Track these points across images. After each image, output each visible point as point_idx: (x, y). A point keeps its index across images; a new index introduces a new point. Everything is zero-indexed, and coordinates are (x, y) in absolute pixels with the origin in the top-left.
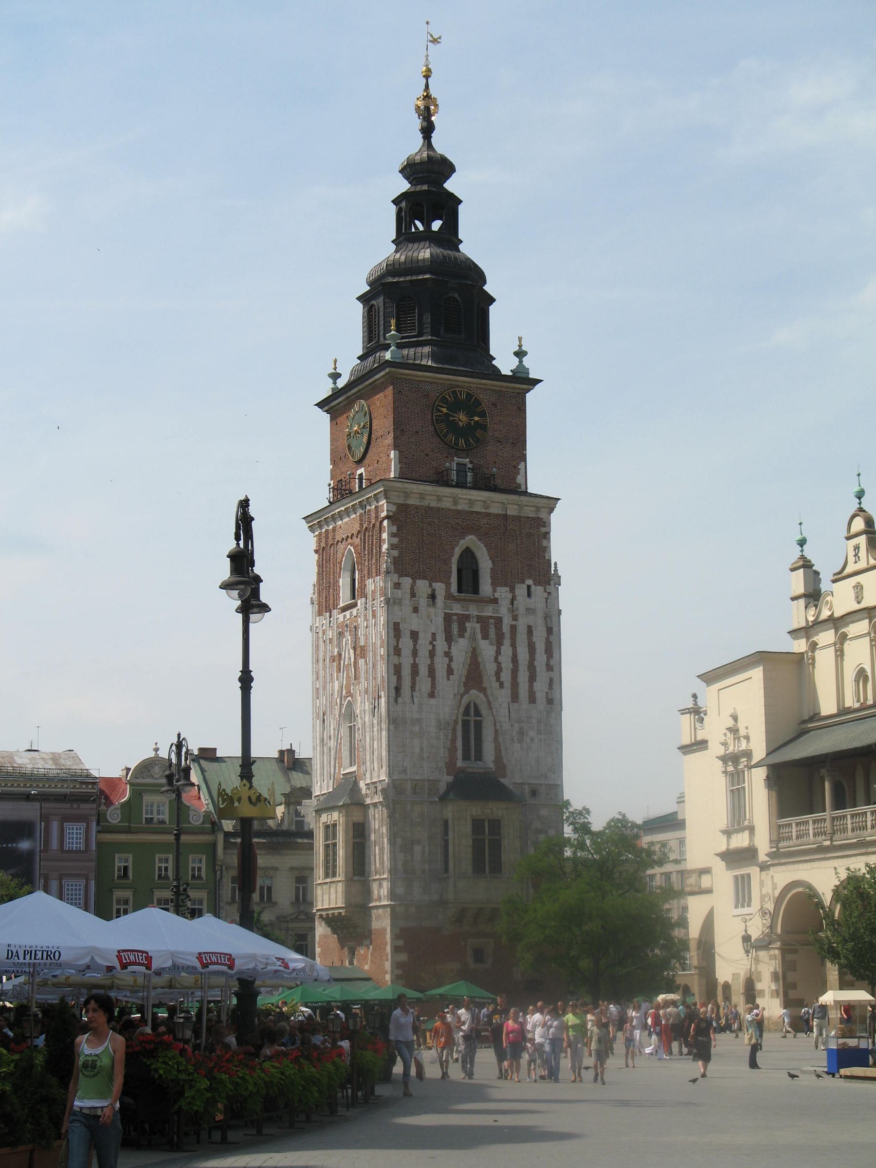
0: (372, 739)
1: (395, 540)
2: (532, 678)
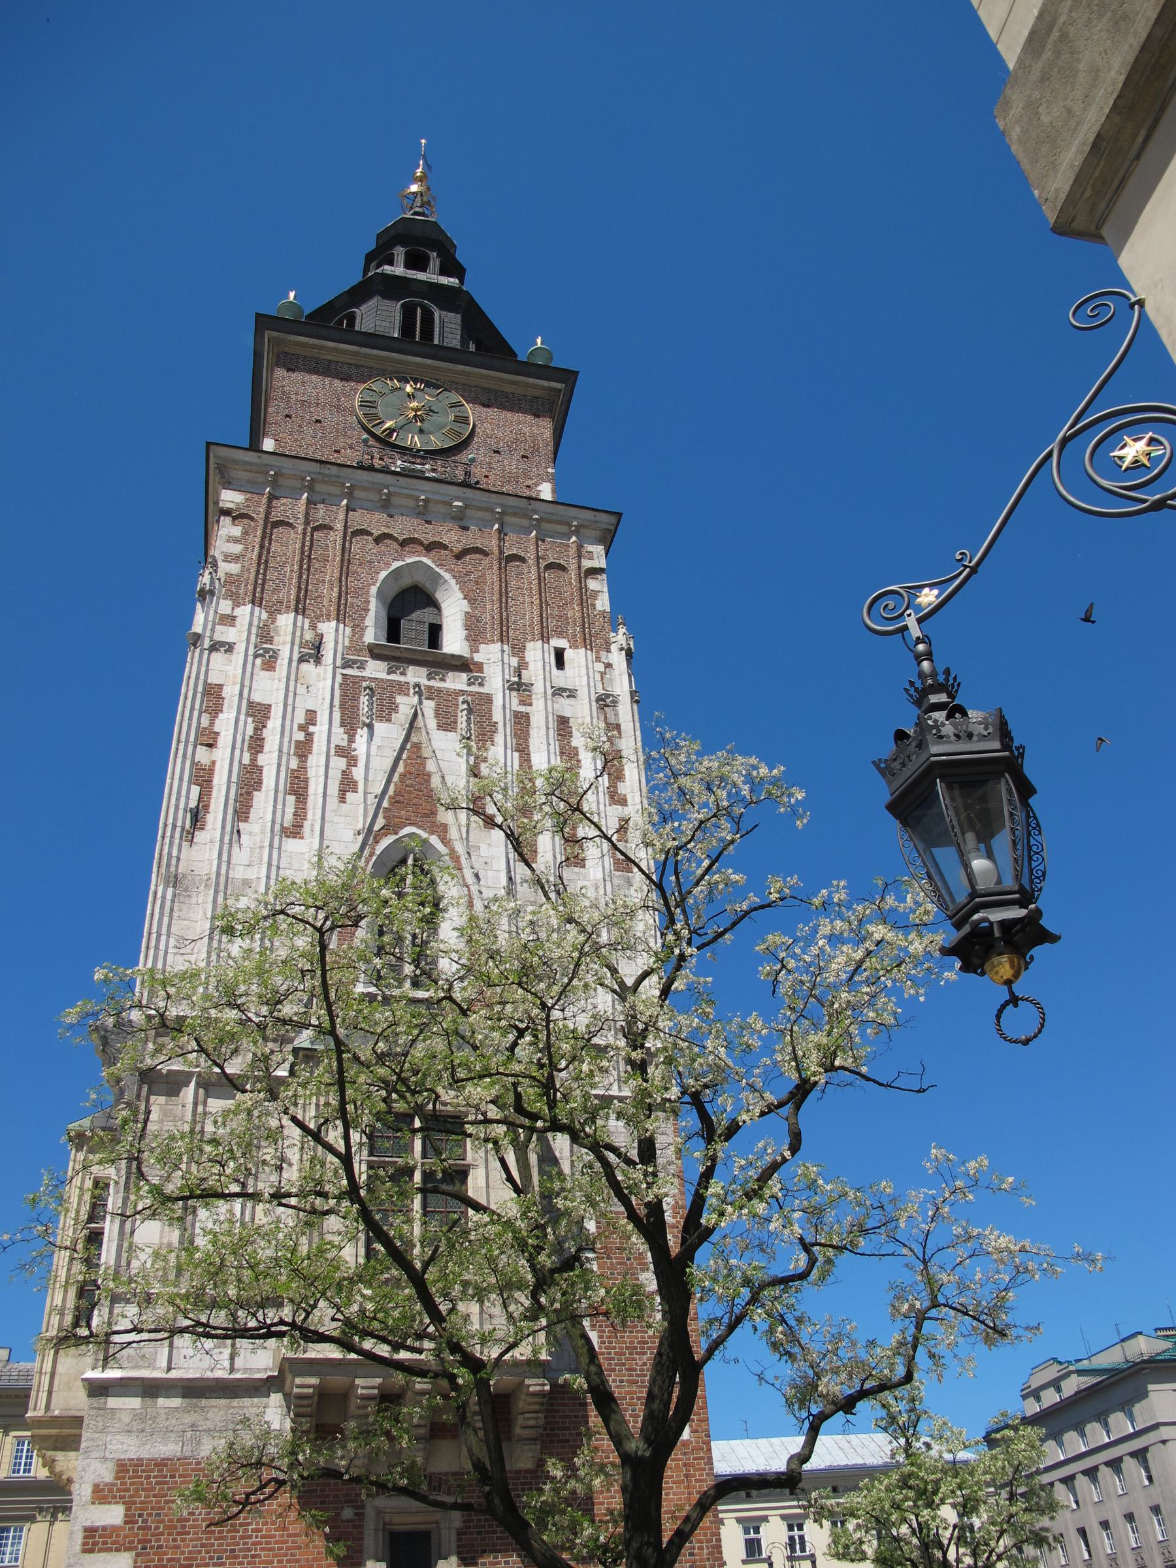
1: (237, 549)
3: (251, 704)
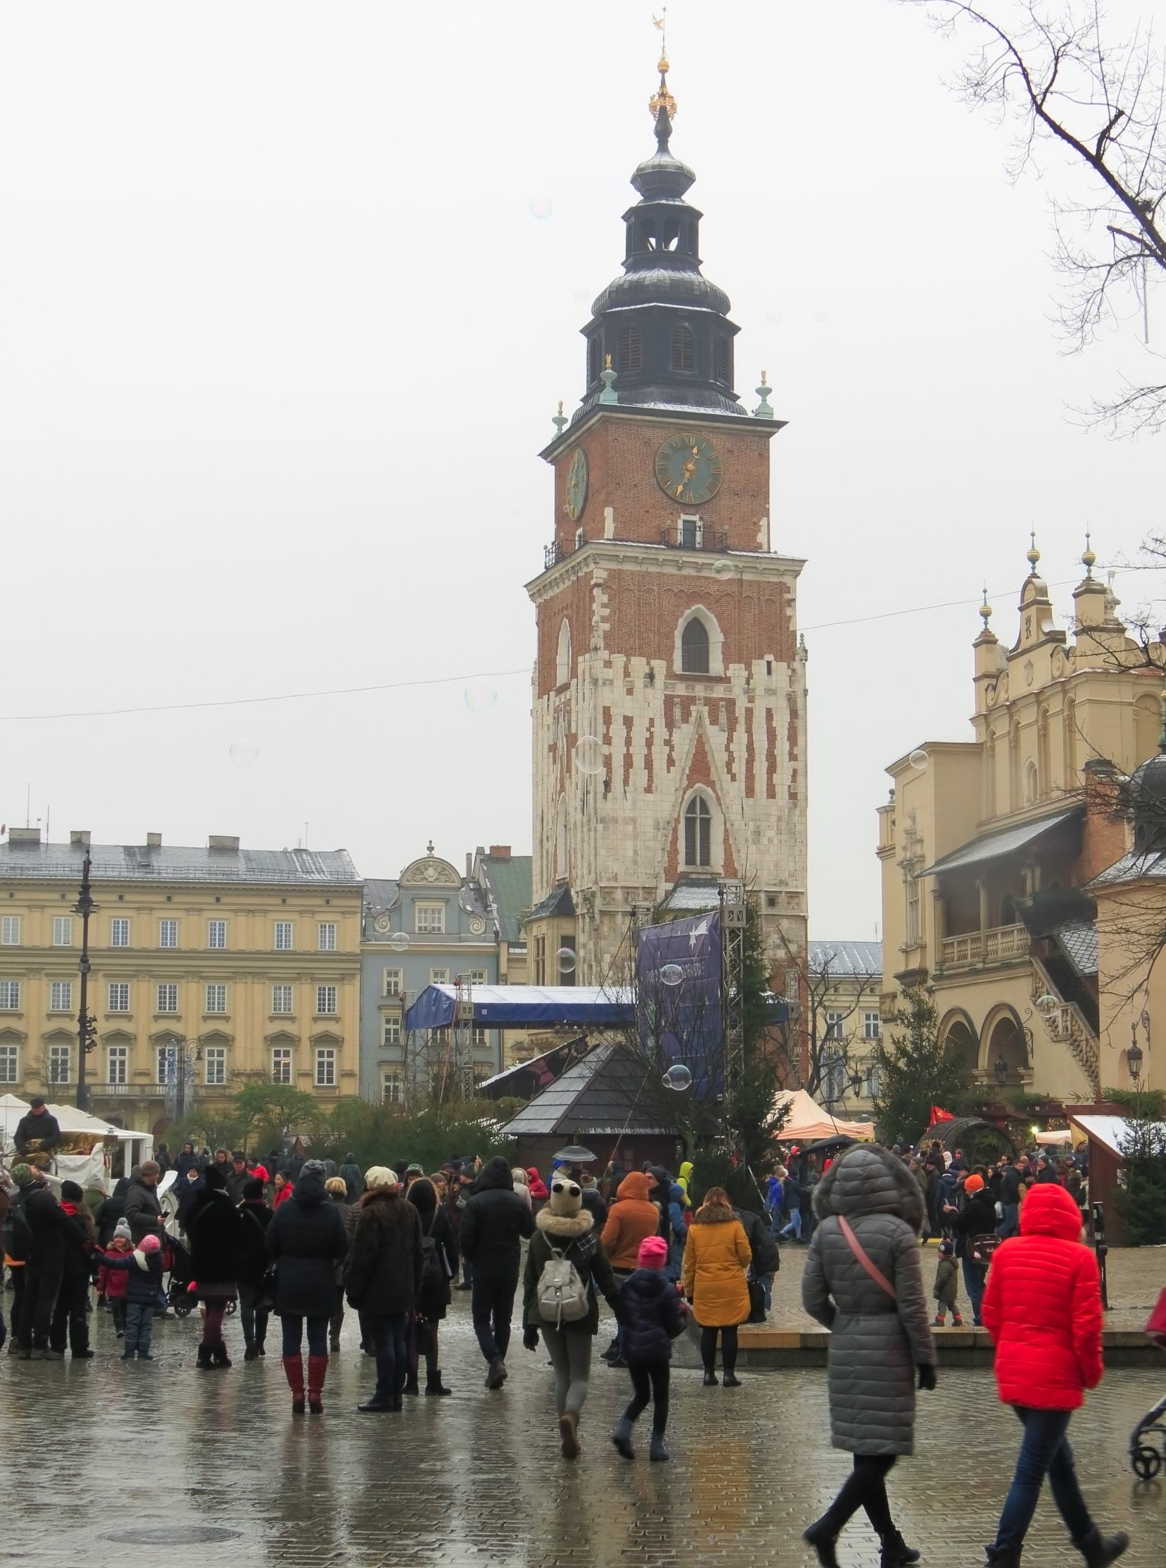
0: (583, 842)
2: (772, 769)
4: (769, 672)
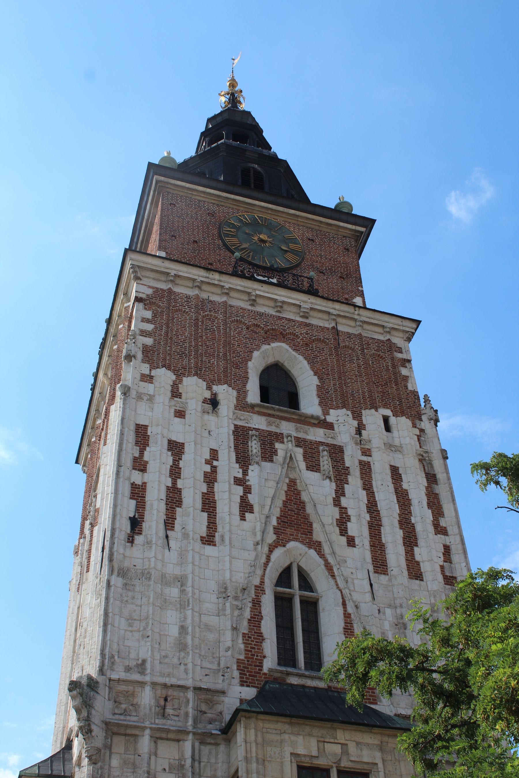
1: (150, 327)
2: (410, 540)
3: (170, 442)
4: (388, 428)
